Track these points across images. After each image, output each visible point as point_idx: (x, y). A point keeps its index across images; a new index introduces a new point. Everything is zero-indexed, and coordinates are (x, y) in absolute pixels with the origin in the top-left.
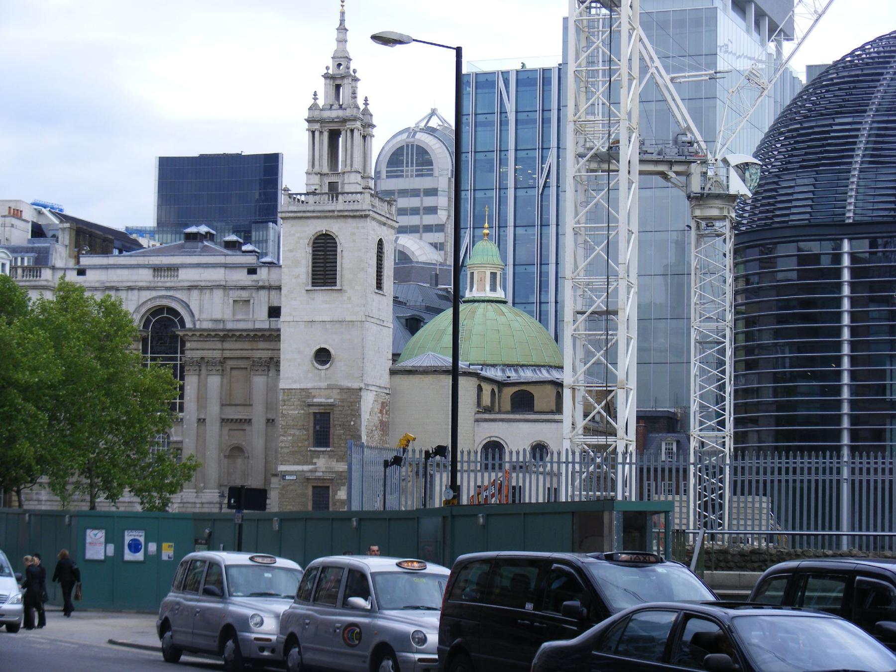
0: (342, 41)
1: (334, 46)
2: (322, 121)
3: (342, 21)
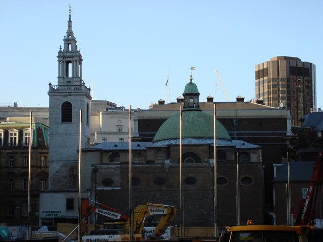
0: (70, 26)
1: (67, 28)
2: (64, 57)
3: (70, 18)
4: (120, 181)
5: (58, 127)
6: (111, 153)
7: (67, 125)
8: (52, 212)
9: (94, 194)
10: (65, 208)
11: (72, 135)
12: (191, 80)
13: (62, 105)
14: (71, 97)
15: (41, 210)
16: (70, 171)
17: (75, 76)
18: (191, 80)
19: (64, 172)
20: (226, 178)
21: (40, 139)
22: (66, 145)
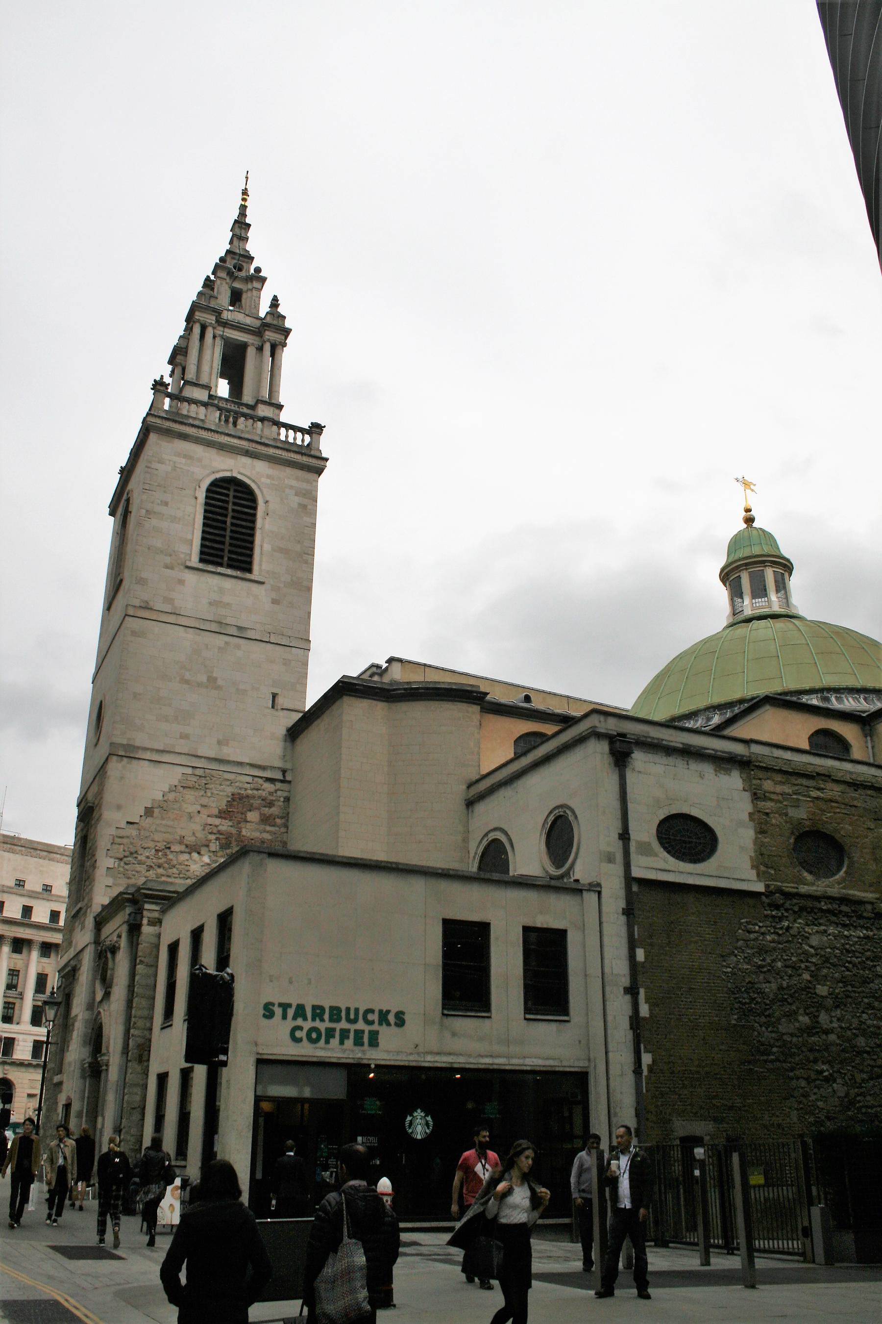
4: (747, 835)
5: (181, 582)
7: (228, 584)
8: (335, 1014)
10: (435, 990)
11: (250, 634)
12: (749, 520)
13: (208, 490)
16: (223, 814)
17: (266, 395)
18: (749, 520)
19: (190, 817)
22: (212, 680)
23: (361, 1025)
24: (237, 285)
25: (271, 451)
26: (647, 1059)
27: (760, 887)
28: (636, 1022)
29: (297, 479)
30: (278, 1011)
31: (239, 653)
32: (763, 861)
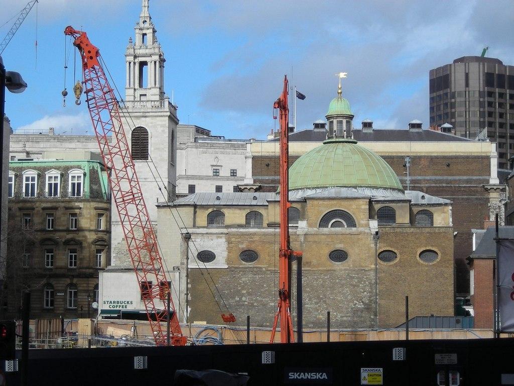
4: (225, 254)
6: (210, 210)
8: (118, 302)
9: (184, 274)
10: (139, 296)
11: (149, 180)
13: (133, 132)
14: (147, 119)
15: (101, 299)
20: (396, 251)
21: (95, 187)
23: (123, 304)
24: (144, 32)
25: (151, 114)
26: (189, 309)
27: (226, 267)
28: (187, 301)
29: (161, 121)
30: (106, 303)
31: (146, 187)
32: (228, 261)
